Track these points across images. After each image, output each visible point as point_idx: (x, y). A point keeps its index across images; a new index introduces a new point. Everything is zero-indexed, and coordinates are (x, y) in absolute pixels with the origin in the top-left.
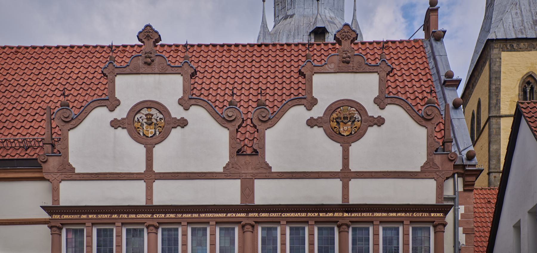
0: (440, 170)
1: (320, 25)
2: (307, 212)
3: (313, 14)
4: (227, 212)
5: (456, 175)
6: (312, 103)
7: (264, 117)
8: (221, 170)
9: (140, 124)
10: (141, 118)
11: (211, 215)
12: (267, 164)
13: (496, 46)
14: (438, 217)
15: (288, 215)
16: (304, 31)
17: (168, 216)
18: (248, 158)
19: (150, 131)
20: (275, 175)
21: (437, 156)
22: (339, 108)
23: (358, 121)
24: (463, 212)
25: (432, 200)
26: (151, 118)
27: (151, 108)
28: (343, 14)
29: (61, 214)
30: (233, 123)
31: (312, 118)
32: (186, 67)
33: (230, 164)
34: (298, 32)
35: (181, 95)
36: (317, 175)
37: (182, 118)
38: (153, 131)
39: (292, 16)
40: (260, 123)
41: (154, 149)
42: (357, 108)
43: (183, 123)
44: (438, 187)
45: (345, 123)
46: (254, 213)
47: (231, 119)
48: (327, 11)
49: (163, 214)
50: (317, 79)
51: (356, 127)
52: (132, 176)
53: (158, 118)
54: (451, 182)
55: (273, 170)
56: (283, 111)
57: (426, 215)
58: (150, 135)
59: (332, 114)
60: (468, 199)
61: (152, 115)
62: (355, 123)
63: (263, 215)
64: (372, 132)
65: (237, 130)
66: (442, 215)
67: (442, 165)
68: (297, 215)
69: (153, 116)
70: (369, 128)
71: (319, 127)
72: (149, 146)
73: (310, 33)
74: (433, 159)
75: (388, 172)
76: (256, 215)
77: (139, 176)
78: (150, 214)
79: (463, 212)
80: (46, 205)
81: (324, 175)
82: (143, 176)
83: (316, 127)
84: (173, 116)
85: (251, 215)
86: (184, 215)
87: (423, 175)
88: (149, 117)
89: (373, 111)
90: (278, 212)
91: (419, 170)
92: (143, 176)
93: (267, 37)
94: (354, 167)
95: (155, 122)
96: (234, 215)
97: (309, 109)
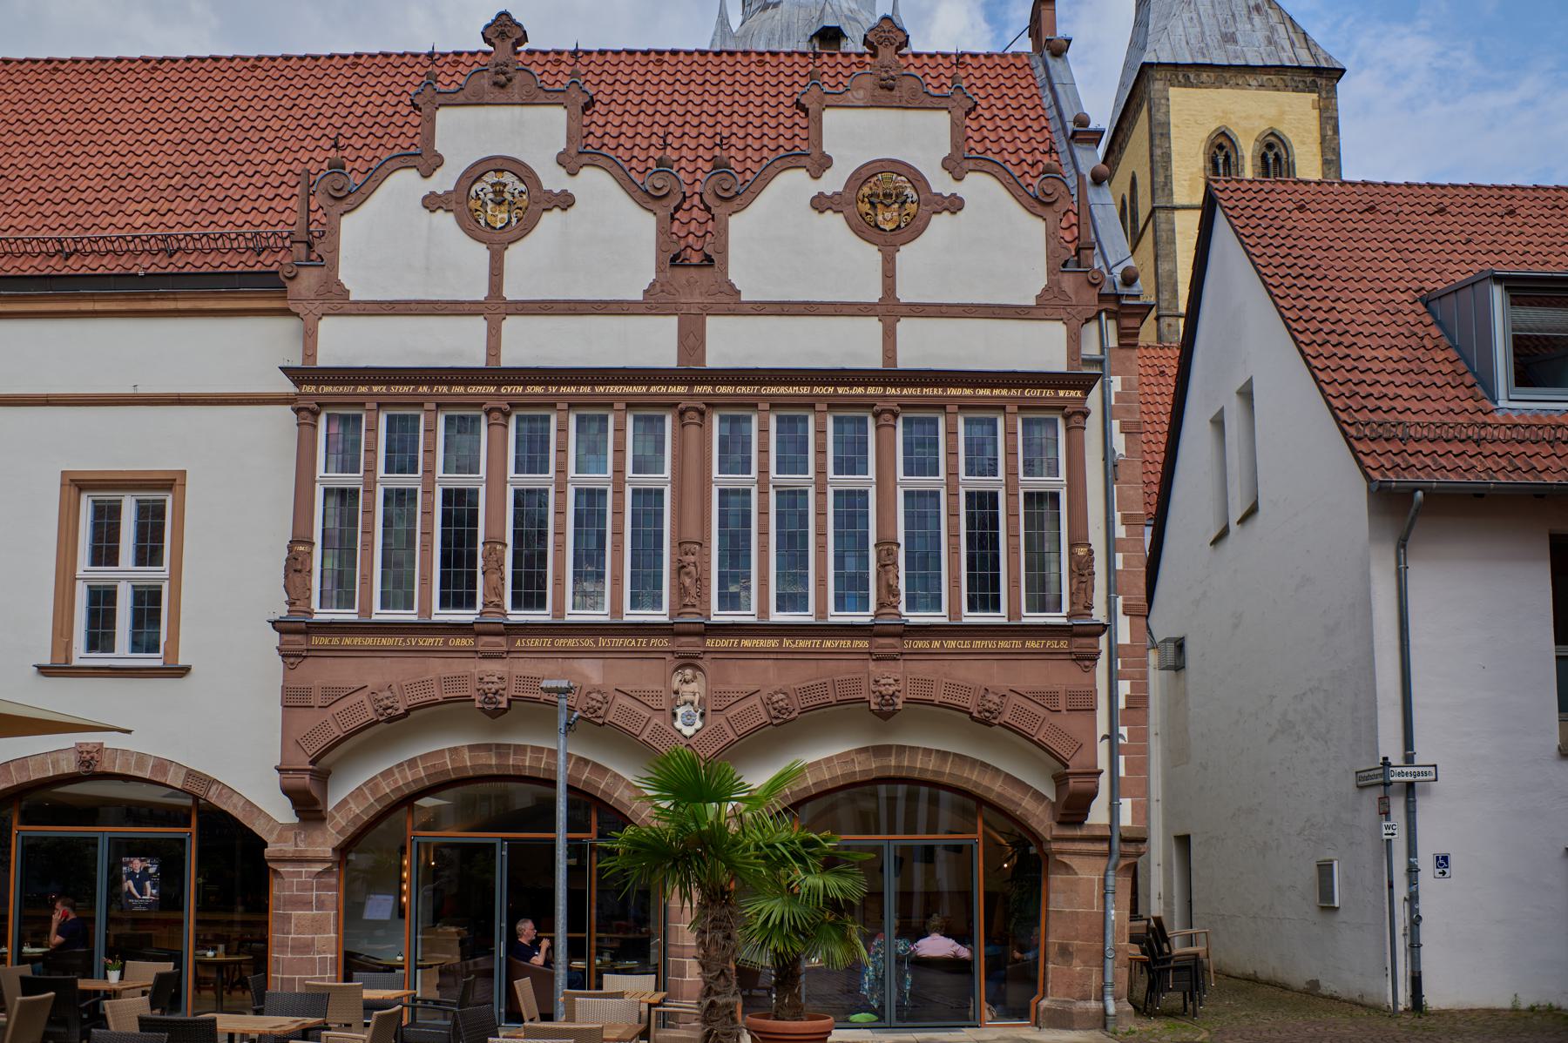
0: (1074, 303)
1: (829, 22)
2: (812, 384)
4: (649, 383)
5: (1103, 315)
6: (821, 165)
7: (727, 190)
8: (640, 297)
9: (480, 202)
10: (482, 190)
11: (616, 388)
12: (732, 286)
13: (1158, 77)
14: (1072, 398)
15: (774, 390)
17: (529, 389)
18: (693, 272)
19: (500, 216)
21: (1066, 276)
22: (875, 175)
23: (912, 202)
24: (1119, 390)
25: (1058, 362)
26: (503, 192)
27: (503, 171)
29: (318, 383)
30: (664, 202)
31: (821, 194)
32: (574, 91)
33: (658, 285)
34: (789, 35)
35: (562, 146)
36: (831, 309)
38: (506, 216)
40: (718, 202)
41: (506, 253)
42: (910, 177)
43: (565, 201)
44: (1069, 337)
46: (704, 385)
49: (520, 385)
50: (830, 118)
51: (908, 214)
52: (459, 307)
53: (516, 192)
54: (1093, 328)
55: (744, 298)
56: (763, 179)
57: (1049, 393)
58: (499, 225)
59: (860, 188)
60: (1128, 364)
61: (505, 185)
62: (907, 205)
63: (723, 390)
64: (940, 224)
65: (672, 215)
66: (1079, 394)
67: (1076, 293)
69: (507, 188)
70: (935, 217)
71: (835, 212)
72: (496, 246)
73: (812, 37)
74: (1059, 282)
75: (973, 305)
76: (709, 389)
77: (474, 307)
78: (493, 385)
79: (1119, 390)
80: (290, 365)
81: (846, 309)
82: (482, 307)
83: (829, 213)
84: (546, 186)
85: (698, 389)
86: (563, 389)
87: (1040, 313)
88: (499, 189)
89: (941, 183)
90: (753, 385)
91: (1032, 302)
92: (482, 307)
94: (905, 294)
95: (511, 199)
96: (664, 389)
97: (816, 176)
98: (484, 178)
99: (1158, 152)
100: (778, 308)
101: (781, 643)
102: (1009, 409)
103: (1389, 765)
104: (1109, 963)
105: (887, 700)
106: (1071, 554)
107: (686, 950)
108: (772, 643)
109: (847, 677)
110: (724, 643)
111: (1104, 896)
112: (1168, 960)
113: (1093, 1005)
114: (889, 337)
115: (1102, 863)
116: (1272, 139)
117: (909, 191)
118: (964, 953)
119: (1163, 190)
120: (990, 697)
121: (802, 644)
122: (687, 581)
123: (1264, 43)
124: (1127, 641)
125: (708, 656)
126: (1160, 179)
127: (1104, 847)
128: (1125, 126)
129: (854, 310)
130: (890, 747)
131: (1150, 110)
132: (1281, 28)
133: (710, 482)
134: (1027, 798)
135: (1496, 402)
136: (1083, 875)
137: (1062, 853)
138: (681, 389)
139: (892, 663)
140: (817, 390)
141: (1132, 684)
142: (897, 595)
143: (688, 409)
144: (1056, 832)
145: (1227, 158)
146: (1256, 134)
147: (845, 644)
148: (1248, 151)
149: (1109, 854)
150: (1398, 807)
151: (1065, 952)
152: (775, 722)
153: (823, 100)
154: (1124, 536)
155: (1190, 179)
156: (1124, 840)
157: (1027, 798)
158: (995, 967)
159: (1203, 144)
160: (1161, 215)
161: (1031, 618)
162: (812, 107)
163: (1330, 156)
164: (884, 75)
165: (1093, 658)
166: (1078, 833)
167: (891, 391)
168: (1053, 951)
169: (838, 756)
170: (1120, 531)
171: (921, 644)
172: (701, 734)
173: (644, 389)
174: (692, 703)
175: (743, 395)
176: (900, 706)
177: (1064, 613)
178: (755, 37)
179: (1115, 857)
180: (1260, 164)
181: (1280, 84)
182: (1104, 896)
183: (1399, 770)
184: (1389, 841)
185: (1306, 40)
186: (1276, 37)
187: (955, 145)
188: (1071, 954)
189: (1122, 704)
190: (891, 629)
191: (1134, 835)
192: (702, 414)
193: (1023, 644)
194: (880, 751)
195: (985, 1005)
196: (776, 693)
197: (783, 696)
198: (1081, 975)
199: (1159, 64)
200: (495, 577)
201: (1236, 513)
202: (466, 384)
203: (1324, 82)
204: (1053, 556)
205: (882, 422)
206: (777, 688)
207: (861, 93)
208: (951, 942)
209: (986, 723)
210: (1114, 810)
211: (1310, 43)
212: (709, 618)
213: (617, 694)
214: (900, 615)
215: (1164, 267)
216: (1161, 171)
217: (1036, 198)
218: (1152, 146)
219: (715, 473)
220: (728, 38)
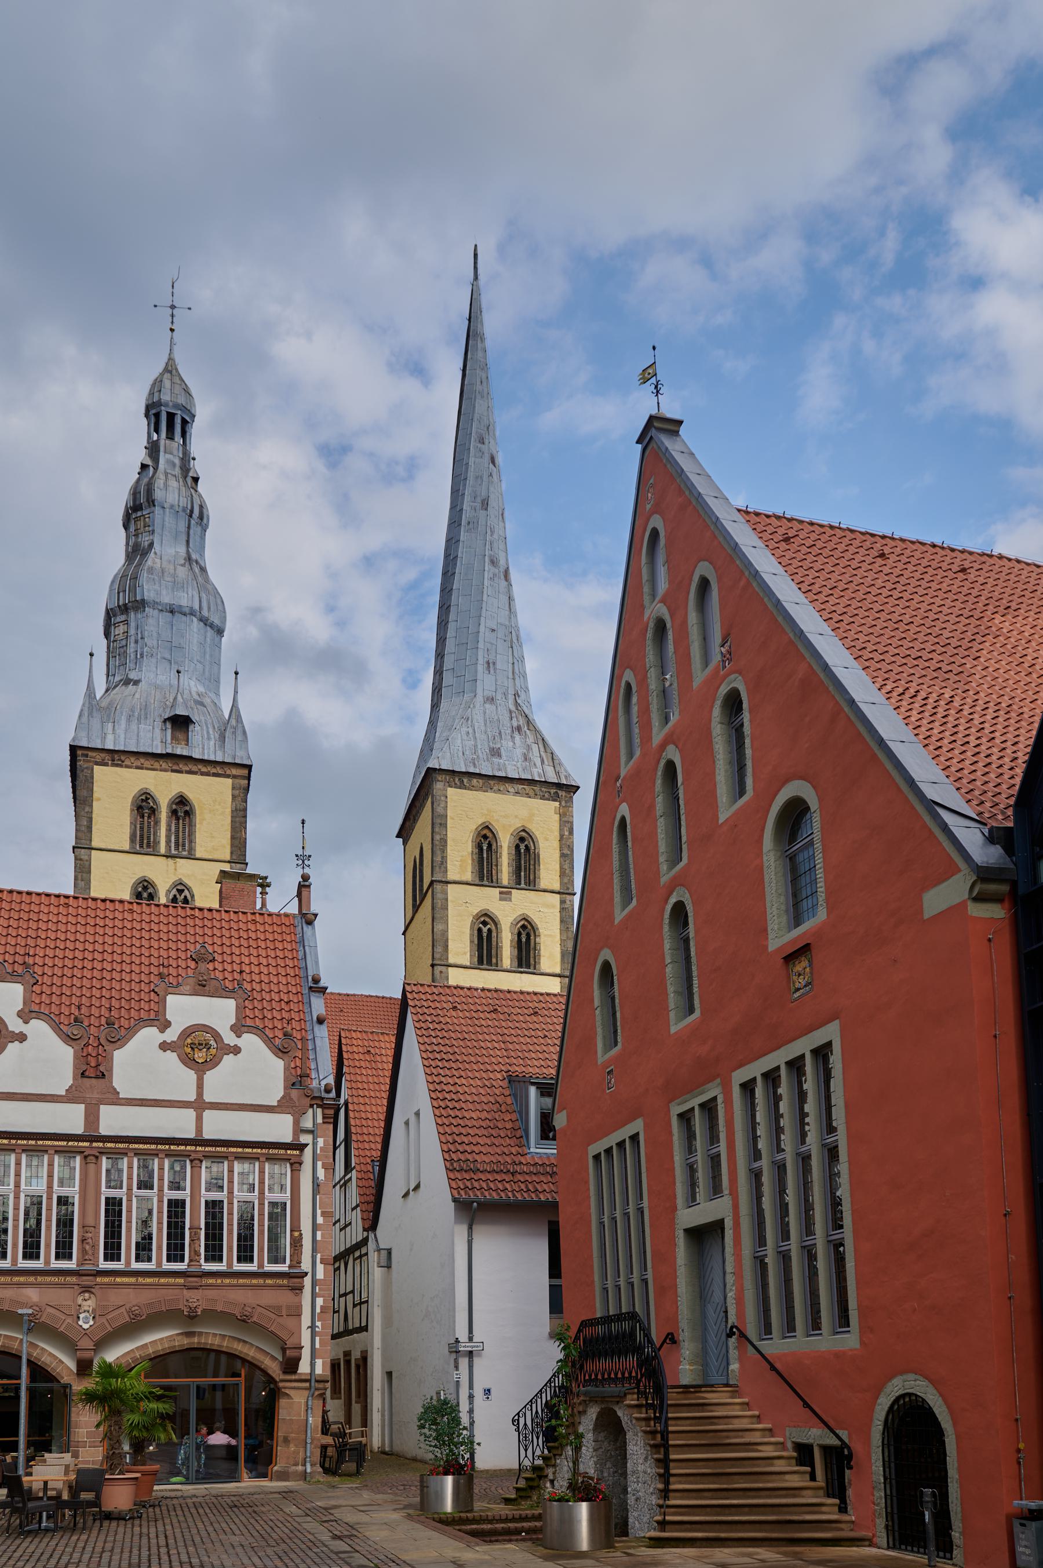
1: (181, 711)
2: (157, 1144)
3: (171, 686)
12: (115, 1089)
13: (440, 779)
15: (136, 1146)
16: (156, 714)
18: (94, 1081)
20: (123, 1101)
21: (293, 1090)
28: (219, 687)
34: (146, 714)
36: (168, 1104)
39: (136, 683)
45: (200, 1050)
48: (192, 683)
63: (109, 1145)
73: (165, 721)
76: (101, 1145)
83: (169, 1051)
85: (95, 1144)
99: (437, 837)
100: (140, 1102)
102: (261, 1159)
104: (308, 1445)
106: (291, 1235)
108: (132, 1280)
111: (307, 1410)
112: (346, 1445)
113: (300, 1468)
114: (199, 1119)
115: (306, 1393)
116: (523, 834)
117: (212, 1042)
118: (234, 1442)
119: (440, 867)
120: (246, 1308)
121: (149, 1280)
123: (521, 758)
126: (438, 859)
127: (307, 1385)
128: (418, 804)
131: (433, 803)
132: (535, 747)
133: (101, 1193)
136: (296, 1400)
137: (285, 1388)
140: (160, 1147)
141: (324, 1301)
142: (199, 1255)
143: (89, 1155)
144: (282, 1377)
145: (490, 845)
146: (512, 830)
147: (171, 1280)
148: (505, 843)
149: (309, 1389)
151: (286, 1440)
155: (461, 861)
156: (317, 1381)
158: (250, 1449)
159: (472, 835)
160: (438, 887)
161: (269, 1268)
163: (566, 851)
164: (201, 979)
165: (301, 1288)
166: (293, 1377)
167: (199, 1148)
168: (280, 1439)
169: (166, 1337)
170: (320, 1220)
171: (211, 1281)
177: (287, 1265)
178: (117, 712)
179: (313, 1390)
180: (514, 852)
181: (531, 793)
182: (307, 1410)
185: (553, 759)
186: (531, 754)
187: (237, 1018)
189: (318, 1310)
192: (97, 1157)
194: (189, 1334)
195: (244, 1471)
197: (137, 1308)
198: (294, 1452)
199: (440, 770)
201: (412, 1187)
203: (564, 794)
204: (283, 1235)
205: (194, 1165)
206: (134, 1303)
207: (188, 988)
208: (226, 1436)
209: (244, 1321)
210: (313, 1365)
211: (556, 762)
212: (98, 1266)
215: (439, 927)
216: (439, 852)
217: (279, 1049)
219: (103, 1188)
220: (94, 710)
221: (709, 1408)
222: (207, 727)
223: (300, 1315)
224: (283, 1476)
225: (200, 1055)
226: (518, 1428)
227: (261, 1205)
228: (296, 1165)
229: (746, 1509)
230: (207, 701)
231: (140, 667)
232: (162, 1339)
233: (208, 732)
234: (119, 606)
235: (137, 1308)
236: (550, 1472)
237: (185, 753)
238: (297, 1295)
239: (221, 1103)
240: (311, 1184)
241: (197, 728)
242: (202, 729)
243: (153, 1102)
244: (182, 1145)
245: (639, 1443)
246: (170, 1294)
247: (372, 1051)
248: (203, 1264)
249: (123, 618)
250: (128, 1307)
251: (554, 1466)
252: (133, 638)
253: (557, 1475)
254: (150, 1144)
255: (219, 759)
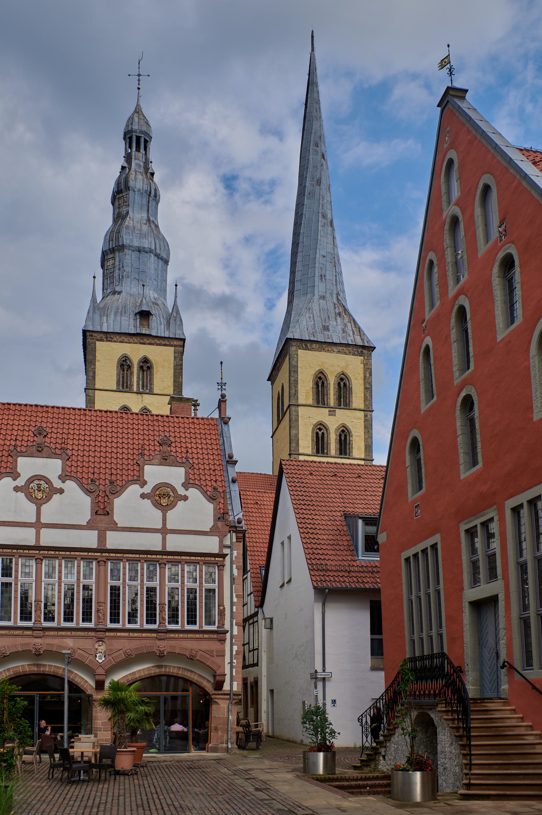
1: (145, 308)
2: (140, 554)
3: (139, 294)
4: (89, 552)
8: (86, 524)
12: (115, 522)
13: (294, 344)
15: (128, 555)
18: (102, 517)
20: (120, 529)
21: (219, 522)
27: (41, 480)
28: (166, 294)
30: (93, 493)
32: (64, 455)
33: (91, 520)
34: (125, 311)
36: (146, 530)
37: (61, 488)
38: (42, 495)
39: (120, 293)
41: (42, 507)
45: (164, 498)
47: (92, 491)
48: (151, 292)
58: (39, 498)
61: (41, 485)
63: (112, 555)
68: (133, 556)
73: (136, 314)
76: (107, 554)
82: (34, 525)
83: (146, 499)
84: (55, 486)
85: (104, 554)
88: (39, 486)
93: (96, 311)
96: (93, 554)
98: (34, 482)
99: (292, 379)
100: (129, 529)
101: (129, 634)
102: (200, 563)
103: (317, 672)
104: (229, 732)
105: (161, 652)
106: (218, 608)
107: (98, 729)
108: (126, 634)
109: (149, 645)
110: (112, 634)
111: (228, 712)
112: (250, 732)
114: (164, 540)
115: (228, 702)
116: (343, 376)
117: (171, 493)
118: (186, 730)
121: (136, 635)
122: (100, 615)
123: (341, 332)
124: (237, 634)
125: (106, 638)
126: (293, 392)
127: (228, 697)
128: (280, 360)
129: (153, 531)
130: (163, 665)
131: (289, 359)
132: (349, 325)
133: (107, 583)
134: (205, 682)
135: (358, 557)
136: (222, 705)
137: (215, 698)
138: (99, 554)
139: (163, 641)
140: (141, 556)
141: (238, 647)
142: (165, 620)
143: (101, 561)
144: (214, 692)
145: (323, 383)
146: (336, 374)
147: (149, 635)
148: (332, 381)
149: (230, 699)
150: (320, 685)
151: (216, 729)
152: (127, 658)
153: (145, 462)
154: (236, 601)
155: (306, 393)
156: (234, 695)
157: (205, 682)
158: (195, 734)
159: (312, 377)
160: (293, 408)
162: (141, 464)
163: (368, 386)
164: (164, 455)
165: (224, 640)
166: (220, 692)
167: (164, 557)
168: (213, 729)
171: (172, 635)
172: (104, 662)
173: (87, 553)
174: (102, 653)
175: (118, 557)
176: (165, 654)
178: (109, 310)
179: (231, 700)
180: (337, 387)
181: (347, 352)
182: (228, 712)
183: (320, 674)
184: (316, 696)
185: (360, 331)
186: (346, 329)
187: (186, 479)
188: (218, 730)
189: (234, 653)
190: (163, 631)
191: (237, 693)
192: (105, 562)
193: (203, 636)
195: (192, 746)
196: (128, 650)
197: (129, 651)
198: (221, 736)
199: (294, 339)
200: (39, 612)
201: (286, 581)
202: (29, 550)
203: (366, 352)
204: (213, 608)
205: (161, 566)
206: (128, 648)
207: (157, 461)
208: (181, 726)
209: (191, 659)
210: (231, 685)
211: (362, 333)
213: (78, 649)
214: (166, 626)
215: (293, 432)
216: (293, 388)
217: (211, 497)
218: (290, 376)
219: (109, 580)
220: (96, 309)
221: (490, 712)
222: (160, 317)
223: (224, 656)
224: (215, 750)
225: (164, 501)
226: (362, 724)
227: (201, 590)
228: (221, 567)
229: (522, 777)
230: (159, 302)
231: (121, 284)
232: (144, 669)
233: (160, 320)
234: (109, 249)
235: (129, 651)
236: (382, 751)
237: (147, 332)
238: (222, 644)
239: (176, 530)
240: (230, 578)
241: (154, 318)
242: (157, 319)
243: (137, 530)
244: (154, 555)
245: (446, 734)
246: (149, 643)
247: (259, 502)
248: (167, 625)
249: (112, 256)
250: (124, 650)
251: (385, 747)
252: (117, 267)
253: (387, 753)
254: (136, 554)
255: (167, 335)
